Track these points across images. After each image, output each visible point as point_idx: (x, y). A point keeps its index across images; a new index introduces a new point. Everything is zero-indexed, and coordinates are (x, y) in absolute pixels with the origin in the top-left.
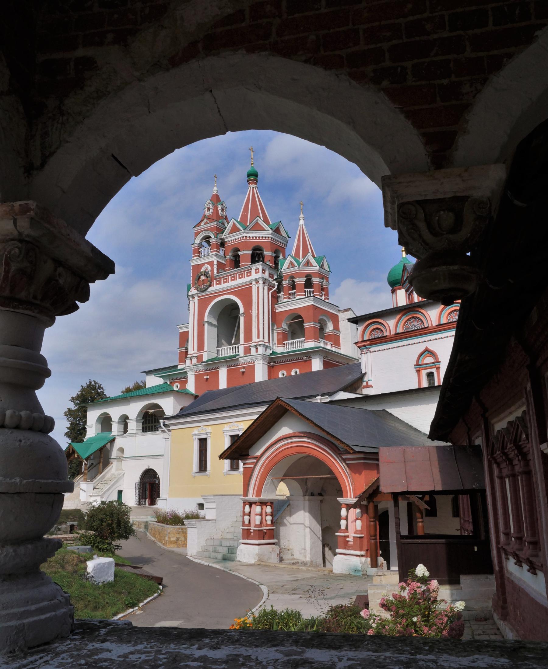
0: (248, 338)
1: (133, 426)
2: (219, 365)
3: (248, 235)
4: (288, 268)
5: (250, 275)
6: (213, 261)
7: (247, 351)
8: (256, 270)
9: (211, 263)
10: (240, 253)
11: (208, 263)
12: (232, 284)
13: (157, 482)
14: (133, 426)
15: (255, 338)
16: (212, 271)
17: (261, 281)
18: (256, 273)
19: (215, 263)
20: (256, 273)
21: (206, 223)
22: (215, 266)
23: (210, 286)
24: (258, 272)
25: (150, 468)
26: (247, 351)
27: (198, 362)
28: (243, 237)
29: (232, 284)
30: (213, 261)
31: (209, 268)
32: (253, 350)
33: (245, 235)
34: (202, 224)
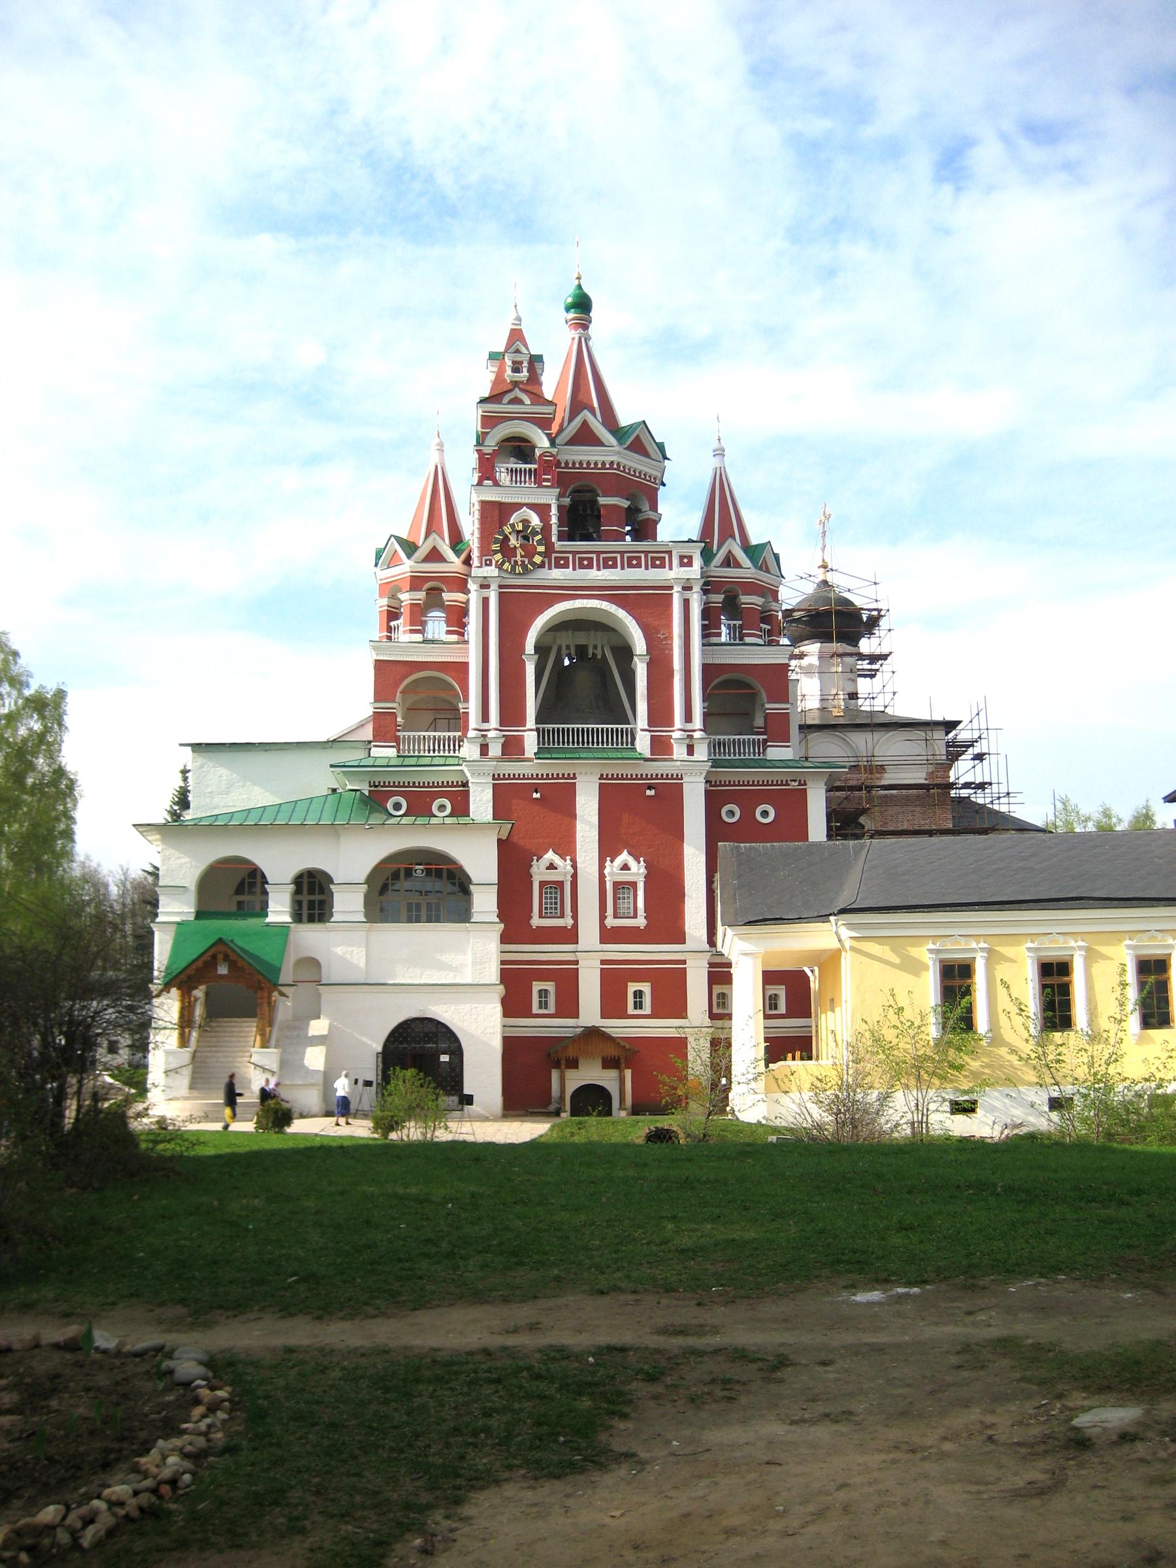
0: (660, 715)
1: (348, 903)
3: (623, 461)
4: (722, 566)
5: (662, 566)
6: (550, 505)
7: (660, 746)
8: (682, 557)
9: (542, 510)
10: (602, 500)
11: (531, 506)
16: (546, 529)
17: (697, 588)
19: (554, 510)
20: (682, 564)
21: (517, 401)
22: (554, 520)
23: (542, 565)
24: (690, 564)
26: (660, 746)
28: (612, 463)
30: (550, 505)
31: (535, 520)
32: (679, 752)
33: (615, 458)
34: (506, 399)
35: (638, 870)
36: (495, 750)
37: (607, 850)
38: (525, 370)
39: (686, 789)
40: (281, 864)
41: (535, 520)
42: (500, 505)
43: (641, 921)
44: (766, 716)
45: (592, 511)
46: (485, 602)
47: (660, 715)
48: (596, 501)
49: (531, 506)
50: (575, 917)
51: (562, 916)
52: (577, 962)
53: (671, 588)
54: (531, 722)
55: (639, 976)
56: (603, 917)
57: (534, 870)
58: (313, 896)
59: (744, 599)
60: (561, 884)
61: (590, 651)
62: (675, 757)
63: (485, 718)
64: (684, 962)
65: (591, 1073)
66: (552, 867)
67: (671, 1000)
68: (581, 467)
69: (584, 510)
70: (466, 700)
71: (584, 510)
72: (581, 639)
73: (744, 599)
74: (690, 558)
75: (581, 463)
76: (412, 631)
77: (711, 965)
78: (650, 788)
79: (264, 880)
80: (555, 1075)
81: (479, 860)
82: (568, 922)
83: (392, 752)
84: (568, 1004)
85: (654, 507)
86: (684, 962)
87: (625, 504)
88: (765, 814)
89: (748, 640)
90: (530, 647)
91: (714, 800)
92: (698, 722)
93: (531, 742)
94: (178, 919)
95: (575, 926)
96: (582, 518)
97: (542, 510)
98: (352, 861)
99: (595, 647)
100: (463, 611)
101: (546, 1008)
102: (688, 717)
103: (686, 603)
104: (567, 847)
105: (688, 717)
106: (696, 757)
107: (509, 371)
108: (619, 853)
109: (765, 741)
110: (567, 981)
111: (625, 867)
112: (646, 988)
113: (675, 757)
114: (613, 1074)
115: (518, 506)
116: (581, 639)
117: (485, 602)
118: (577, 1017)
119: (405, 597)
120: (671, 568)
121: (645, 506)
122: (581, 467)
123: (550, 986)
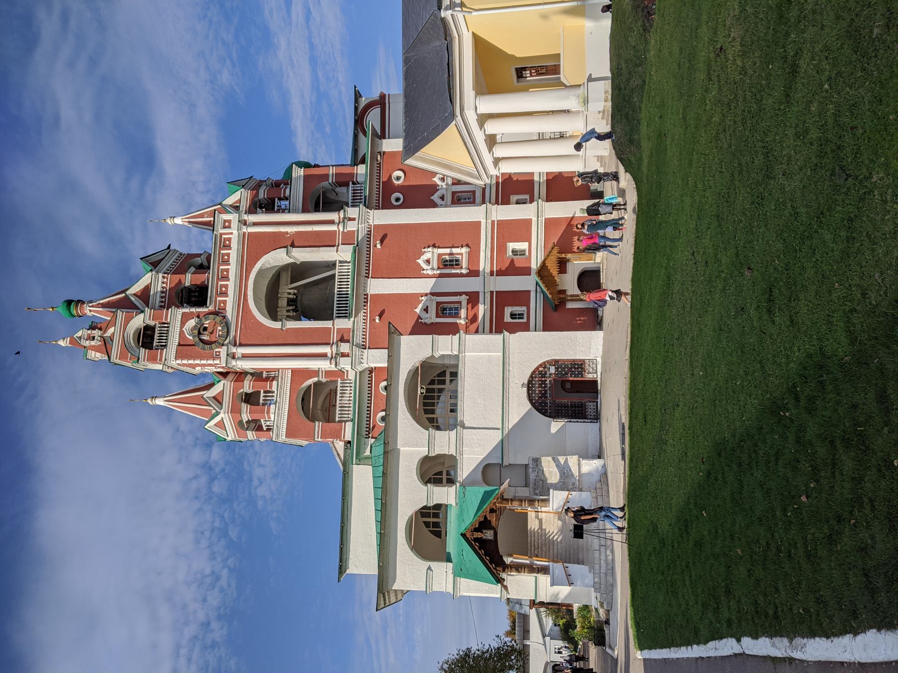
1: (443, 443)
2: (361, 292)
5: (229, 240)
6: (183, 313)
8: (224, 227)
9: (185, 318)
11: (183, 324)
12: (233, 268)
13: (553, 370)
14: (443, 443)
15: (333, 228)
18: (229, 227)
19: (187, 310)
22: (193, 310)
24: (229, 221)
25: (526, 382)
26: (348, 238)
27: (348, 341)
29: (233, 268)
31: (192, 323)
32: (351, 227)
35: (430, 254)
36: (345, 348)
37: (416, 273)
38: (93, 332)
39: (377, 222)
40: (412, 495)
41: (192, 323)
42: (179, 345)
43: (464, 250)
44: (341, 184)
45: (196, 291)
46: (245, 357)
47: (326, 240)
48: (189, 290)
49: (183, 324)
50: (460, 294)
51: (460, 303)
52: (492, 292)
53: (244, 233)
54: (327, 324)
55: (502, 249)
56: (461, 275)
57: (428, 321)
58: (437, 471)
59: (261, 196)
60: (438, 304)
61: (291, 296)
62: (355, 229)
63: (323, 356)
64: (493, 222)
65: (569, 283)
66: (426, 310)
67: (521, 229)
68: (165, 297)
69: (195, 296)
70: (315, 373)
71: (195, 296)
72: (283, 302)
73: (261, 196)
74: (225, 221)
75: (162, 297)
76: (268, 413)
77: (497, 203)
78: (375, 246)
79: (425, 508)
80: (570, 305)
81: (415, 350)
82: (464, 299)
83: (349, 426)
84: (521, 297)
85: (199, 255)
86: (493, 222)
87: (193, 269)
88: (398, 178)
89: (287, 193)
90: (277, 325)
91: (386, 204)
92: (333, 216)
93: (342, 324)
94: (451, 576)
95: (466, 293)
96: (196, 296)
97: (185, 318)
98: (413, 442)
99: (289, 294)
100: (257, 376)
101: (523, 314)
102: (332, 222)
103: (255, 224)
104: (413, 298)
105: (332, 222)
106: (356, 216)
107: (93, 343)
108: (419, 264)
109: (354, 183)
110: (502, 299)
111: (428, 262)
112: (511, 246)
113: (355, 229)
114: (569, 266)
115: (182, 333)
116: (283, 302)
117: (245, 357)
118: (529, 291)
119: (245, 417)
120: (232, 233)
121: (199, 260)
122: (165, 297)
123: (508, 310)
